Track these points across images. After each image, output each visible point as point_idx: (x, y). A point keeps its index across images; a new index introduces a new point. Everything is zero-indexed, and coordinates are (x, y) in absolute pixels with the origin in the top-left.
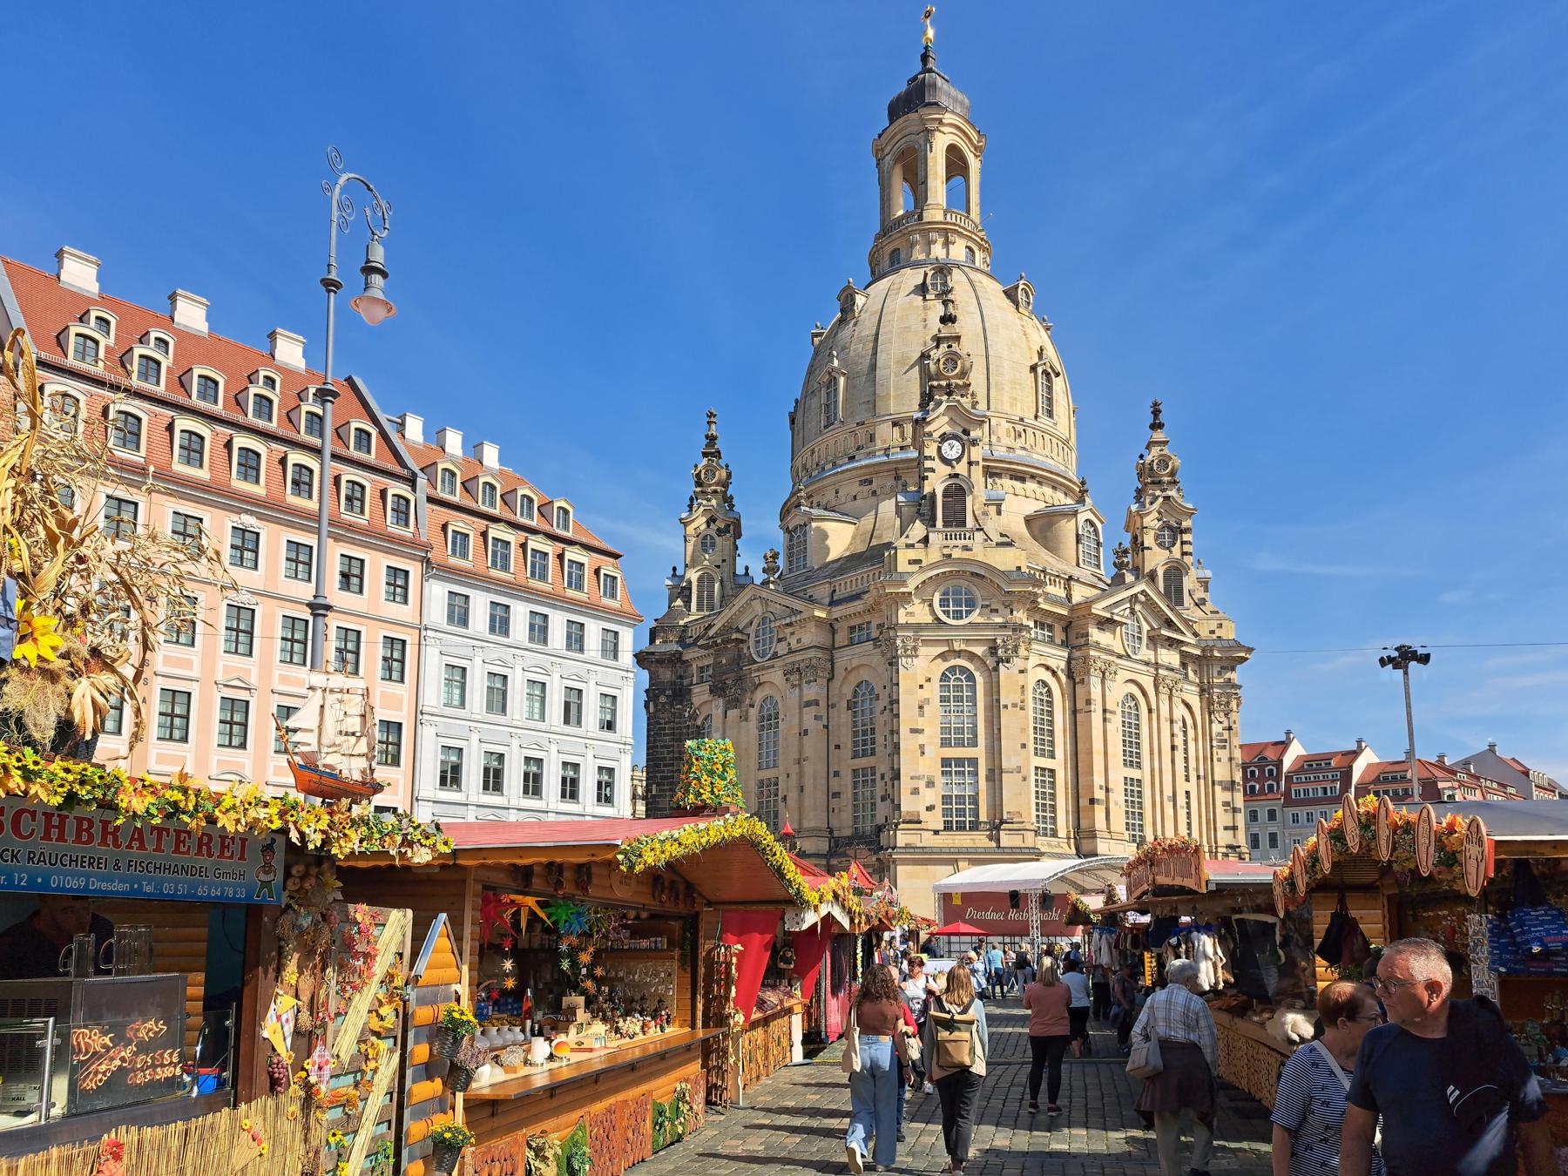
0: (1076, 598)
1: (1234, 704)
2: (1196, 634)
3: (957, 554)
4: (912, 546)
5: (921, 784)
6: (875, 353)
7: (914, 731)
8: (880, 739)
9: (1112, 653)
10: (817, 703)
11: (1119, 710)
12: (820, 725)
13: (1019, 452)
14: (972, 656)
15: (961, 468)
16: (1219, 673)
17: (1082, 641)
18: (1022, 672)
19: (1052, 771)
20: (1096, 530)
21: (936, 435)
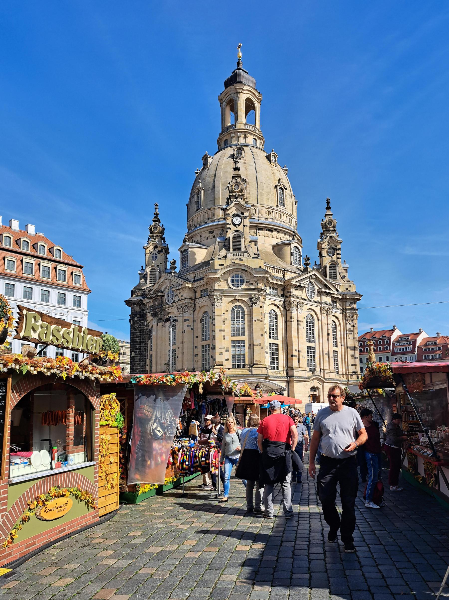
0: (287, 277)
1: (355, 317)
2: (337, 290)
3: (237, 262)
4: (220, 259)
5: (223, 351)
6: (214, 181)
7: (221, 331)
8: (211, 334)
9: (301, 298)
10: (188, 320)
13: (270, 220)
14: (243, 301)
15: (240, 228)
18: (261, 307)
19: (277, 344)
20: (299, 250)
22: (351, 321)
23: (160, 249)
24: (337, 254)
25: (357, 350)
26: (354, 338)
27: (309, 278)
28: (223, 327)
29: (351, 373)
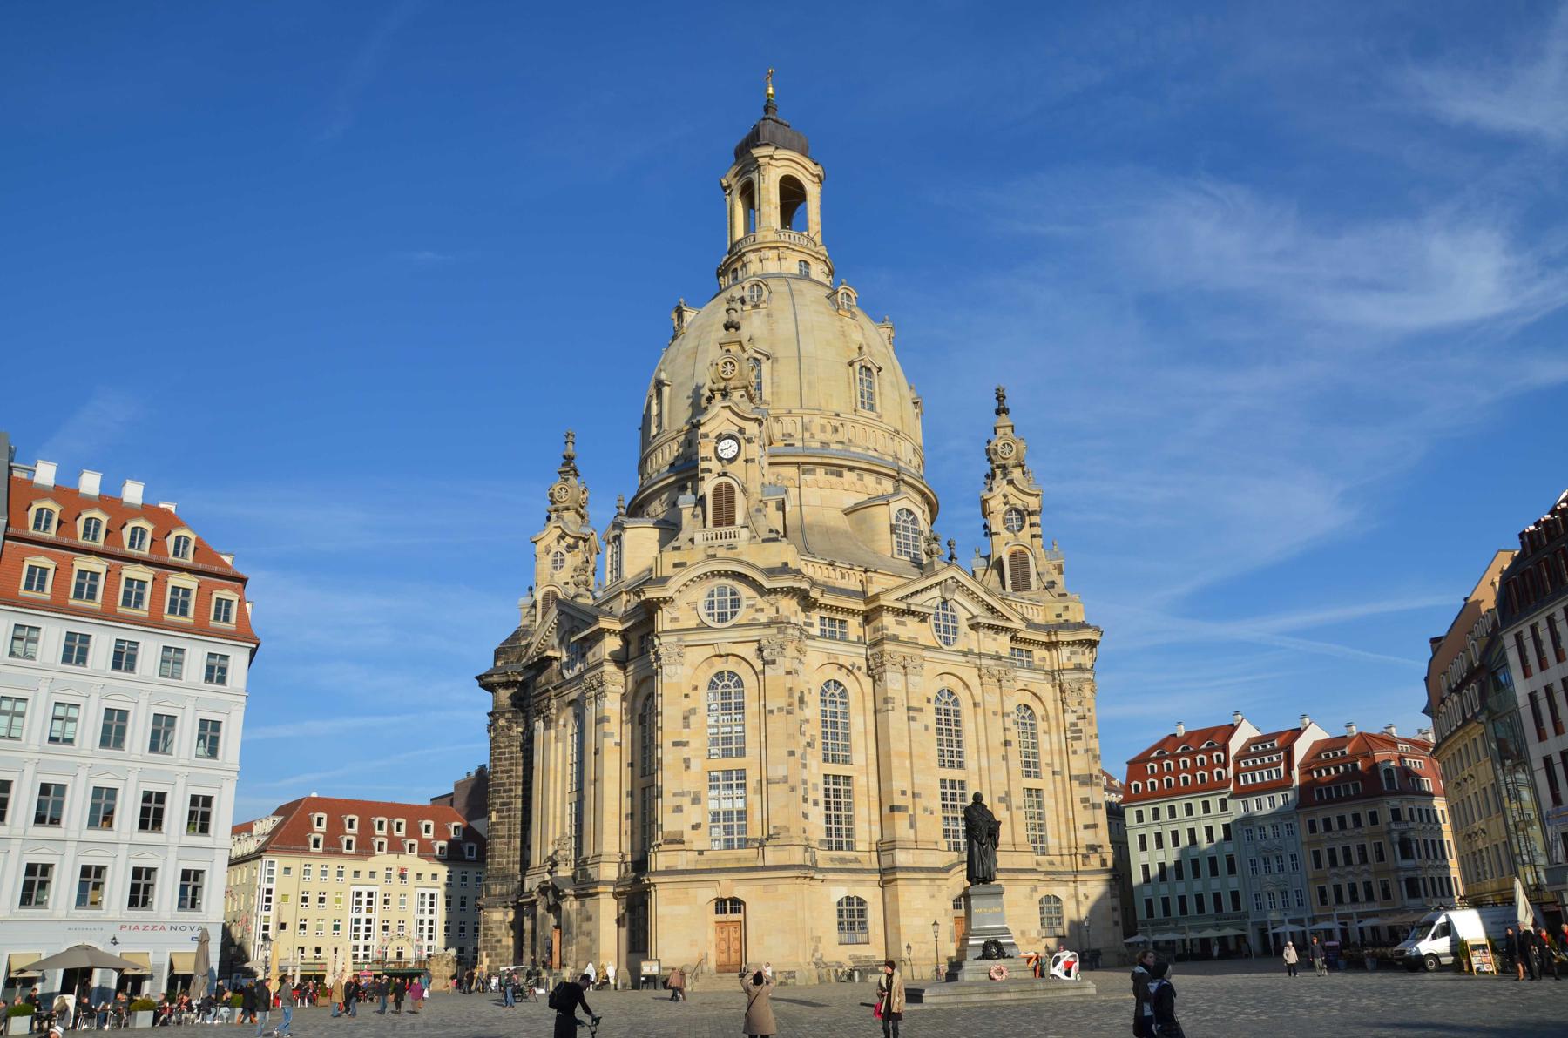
2: (1024, 619)
3: (721, 553)
5: (686, 802)
7: (676, 744)
11: (932, 706)
16: (1069, 659)
17: (879, 635)
18: (789, 673)
19: (847, 778)
21: (713, 435)
26: (1087, 751)
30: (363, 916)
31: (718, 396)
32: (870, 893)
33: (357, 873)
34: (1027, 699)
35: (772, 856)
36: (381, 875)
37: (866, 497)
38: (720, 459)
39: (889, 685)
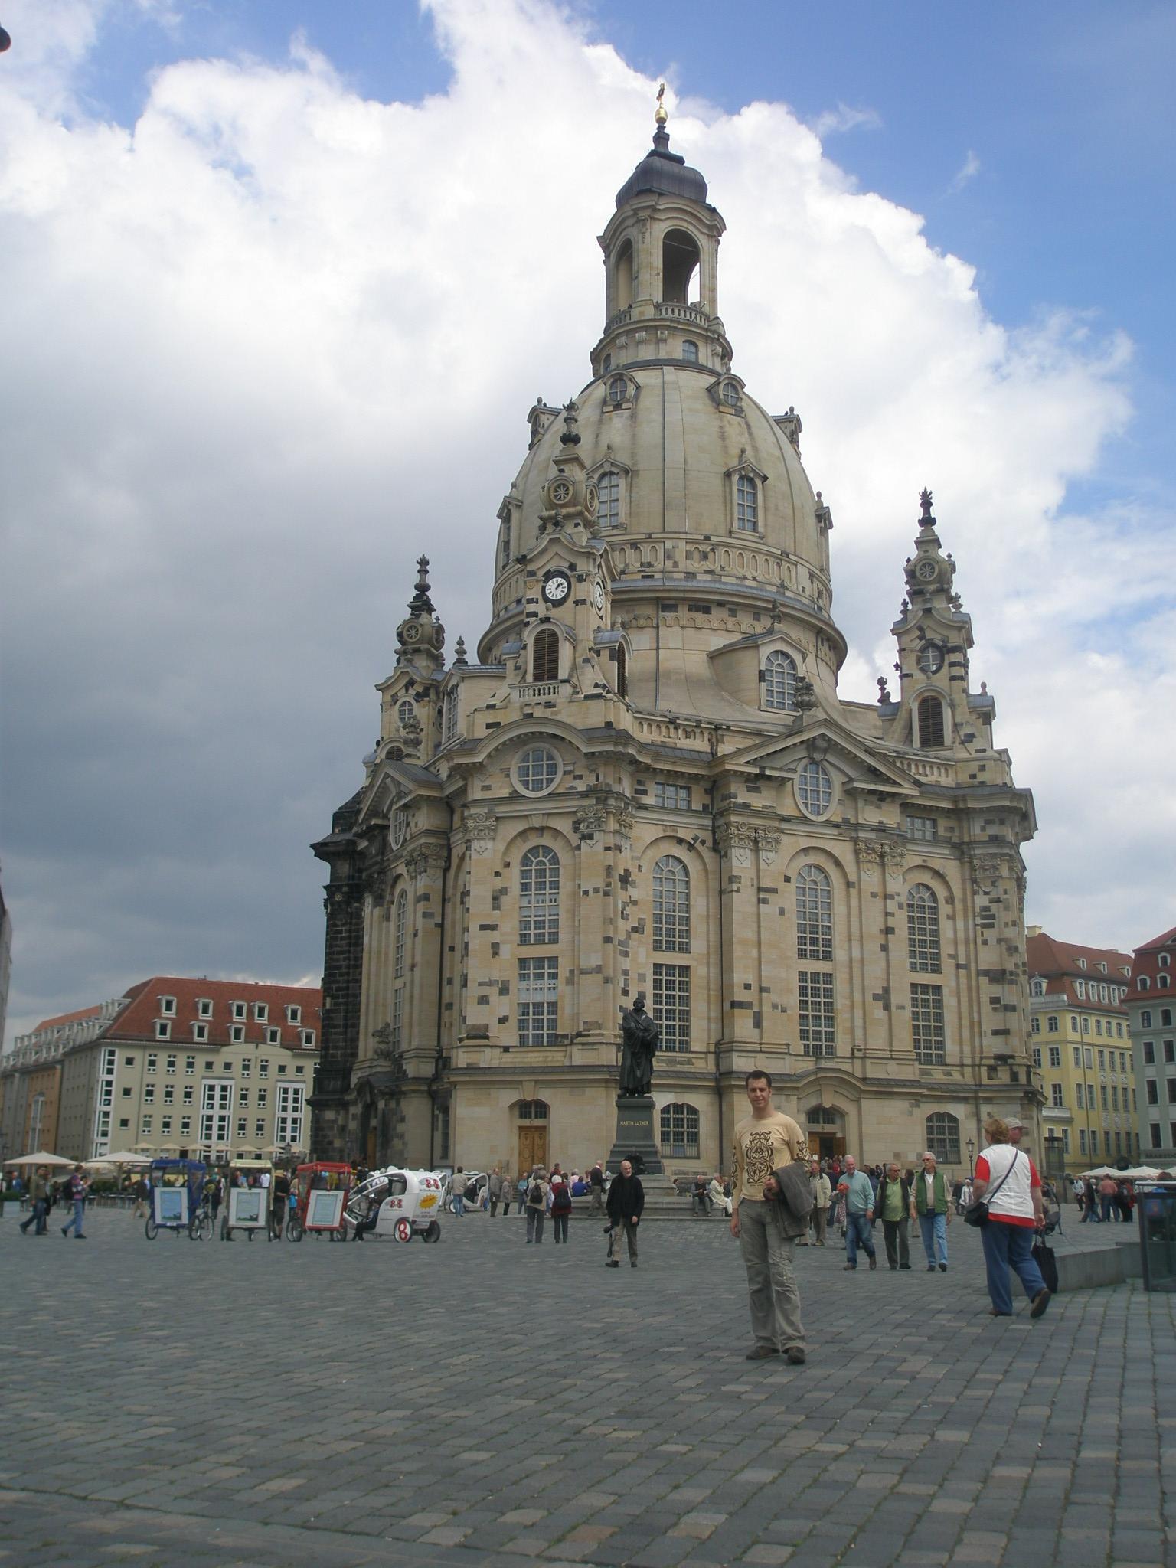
0: (724, 749)
2: (917, 783)
5: (493, 992)
7: (483, 928)
11: (792, 887)
12: (431, 923)
14: (556, 832)
16: (983, 829)
18: (607, 849)
19: (685, 970)
20: (793, 663)
22: (989, 883)
23: (420, 690)
24: (952, 665)
25: (1011, 982)
26: (999, 941)
27: (808, 749)
28: (494, 917)
29: (992, 1062)
30: (216, 1112)
31: (550, 528)
32: (700, 1101)
33: (209, 1065)
34: (926, 878)
35: (579, 1057)
36: (237, 1067)
37: (739, 637)
38: (546, 600)
39: (734, 861)
